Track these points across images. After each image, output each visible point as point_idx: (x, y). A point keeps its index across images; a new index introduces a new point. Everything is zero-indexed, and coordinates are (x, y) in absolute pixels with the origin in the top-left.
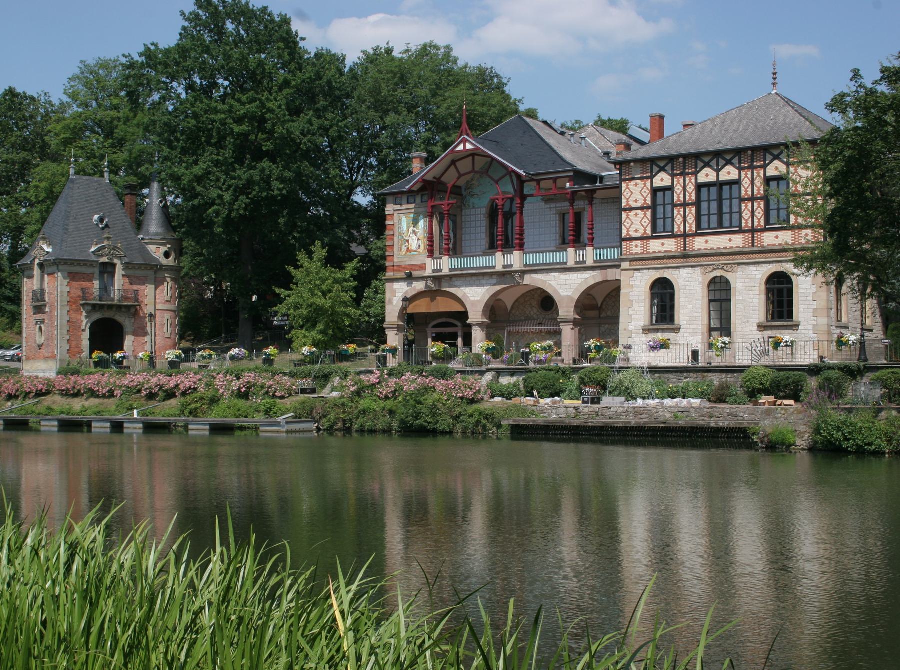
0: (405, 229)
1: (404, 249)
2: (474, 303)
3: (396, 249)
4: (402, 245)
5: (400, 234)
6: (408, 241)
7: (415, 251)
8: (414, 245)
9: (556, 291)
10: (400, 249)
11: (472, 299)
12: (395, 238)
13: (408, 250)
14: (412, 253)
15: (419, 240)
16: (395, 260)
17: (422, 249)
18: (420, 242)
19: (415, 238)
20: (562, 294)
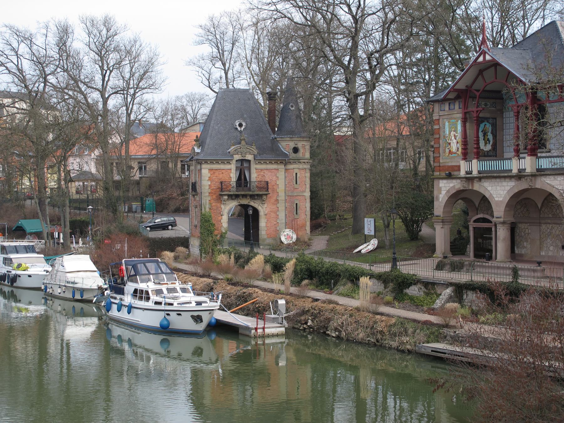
0: (448, 133)
1: (447, 151)
2: (498, 203)
4: (445, 147)
5: (444, 137)
6: (450, 144)
7: (455, 153)
11: (496, 199)
12: (441, 141)
13: (450, 152)
14: (453, 155)
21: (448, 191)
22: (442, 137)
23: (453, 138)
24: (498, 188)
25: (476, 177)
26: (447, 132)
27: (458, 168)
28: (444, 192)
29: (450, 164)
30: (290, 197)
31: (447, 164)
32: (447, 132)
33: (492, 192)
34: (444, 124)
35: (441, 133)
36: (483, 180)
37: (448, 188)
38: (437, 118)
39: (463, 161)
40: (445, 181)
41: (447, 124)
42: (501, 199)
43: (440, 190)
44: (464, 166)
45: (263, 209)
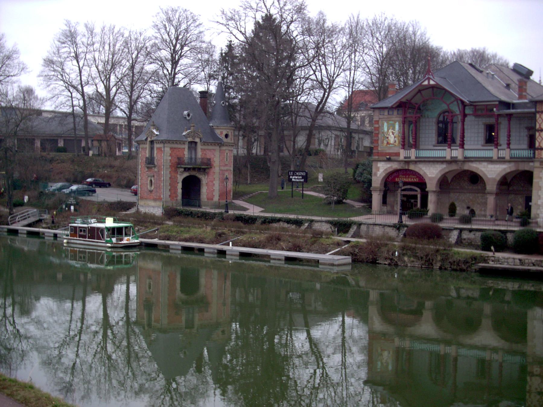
1: (385, 142)
2: (431, 179)
3: (379, 142)
4: (384, 140)
5: (383, 133)
6: (388, 138)
8: (392, 139)
9: (485, 174)
10: (383, 143)
11: (430, 176)
12: (380, 136)
13: (388, 143)
14: (391, 145)
16: (379, 149)
18: (396, 139)
19: (392, 136)
20: (489, 176)
21: (386, 170)
23: (391, 134)
24: (431, 169)
26: (386, 129)
27: (398, 154)
28: (381, 170)
29: (388, 151)
30: (222, 172)
32: (386, 129)
33: (426, 171)
35: (381, 131)
36: (418, 163)
37: (385, 168)
38: (378, 119)
39: (403, 150)
40: (383, 163)
41: (385, 124)
42: (434, 176)
43: (378, 169)
44: (403, 154)
45: (204, 179)
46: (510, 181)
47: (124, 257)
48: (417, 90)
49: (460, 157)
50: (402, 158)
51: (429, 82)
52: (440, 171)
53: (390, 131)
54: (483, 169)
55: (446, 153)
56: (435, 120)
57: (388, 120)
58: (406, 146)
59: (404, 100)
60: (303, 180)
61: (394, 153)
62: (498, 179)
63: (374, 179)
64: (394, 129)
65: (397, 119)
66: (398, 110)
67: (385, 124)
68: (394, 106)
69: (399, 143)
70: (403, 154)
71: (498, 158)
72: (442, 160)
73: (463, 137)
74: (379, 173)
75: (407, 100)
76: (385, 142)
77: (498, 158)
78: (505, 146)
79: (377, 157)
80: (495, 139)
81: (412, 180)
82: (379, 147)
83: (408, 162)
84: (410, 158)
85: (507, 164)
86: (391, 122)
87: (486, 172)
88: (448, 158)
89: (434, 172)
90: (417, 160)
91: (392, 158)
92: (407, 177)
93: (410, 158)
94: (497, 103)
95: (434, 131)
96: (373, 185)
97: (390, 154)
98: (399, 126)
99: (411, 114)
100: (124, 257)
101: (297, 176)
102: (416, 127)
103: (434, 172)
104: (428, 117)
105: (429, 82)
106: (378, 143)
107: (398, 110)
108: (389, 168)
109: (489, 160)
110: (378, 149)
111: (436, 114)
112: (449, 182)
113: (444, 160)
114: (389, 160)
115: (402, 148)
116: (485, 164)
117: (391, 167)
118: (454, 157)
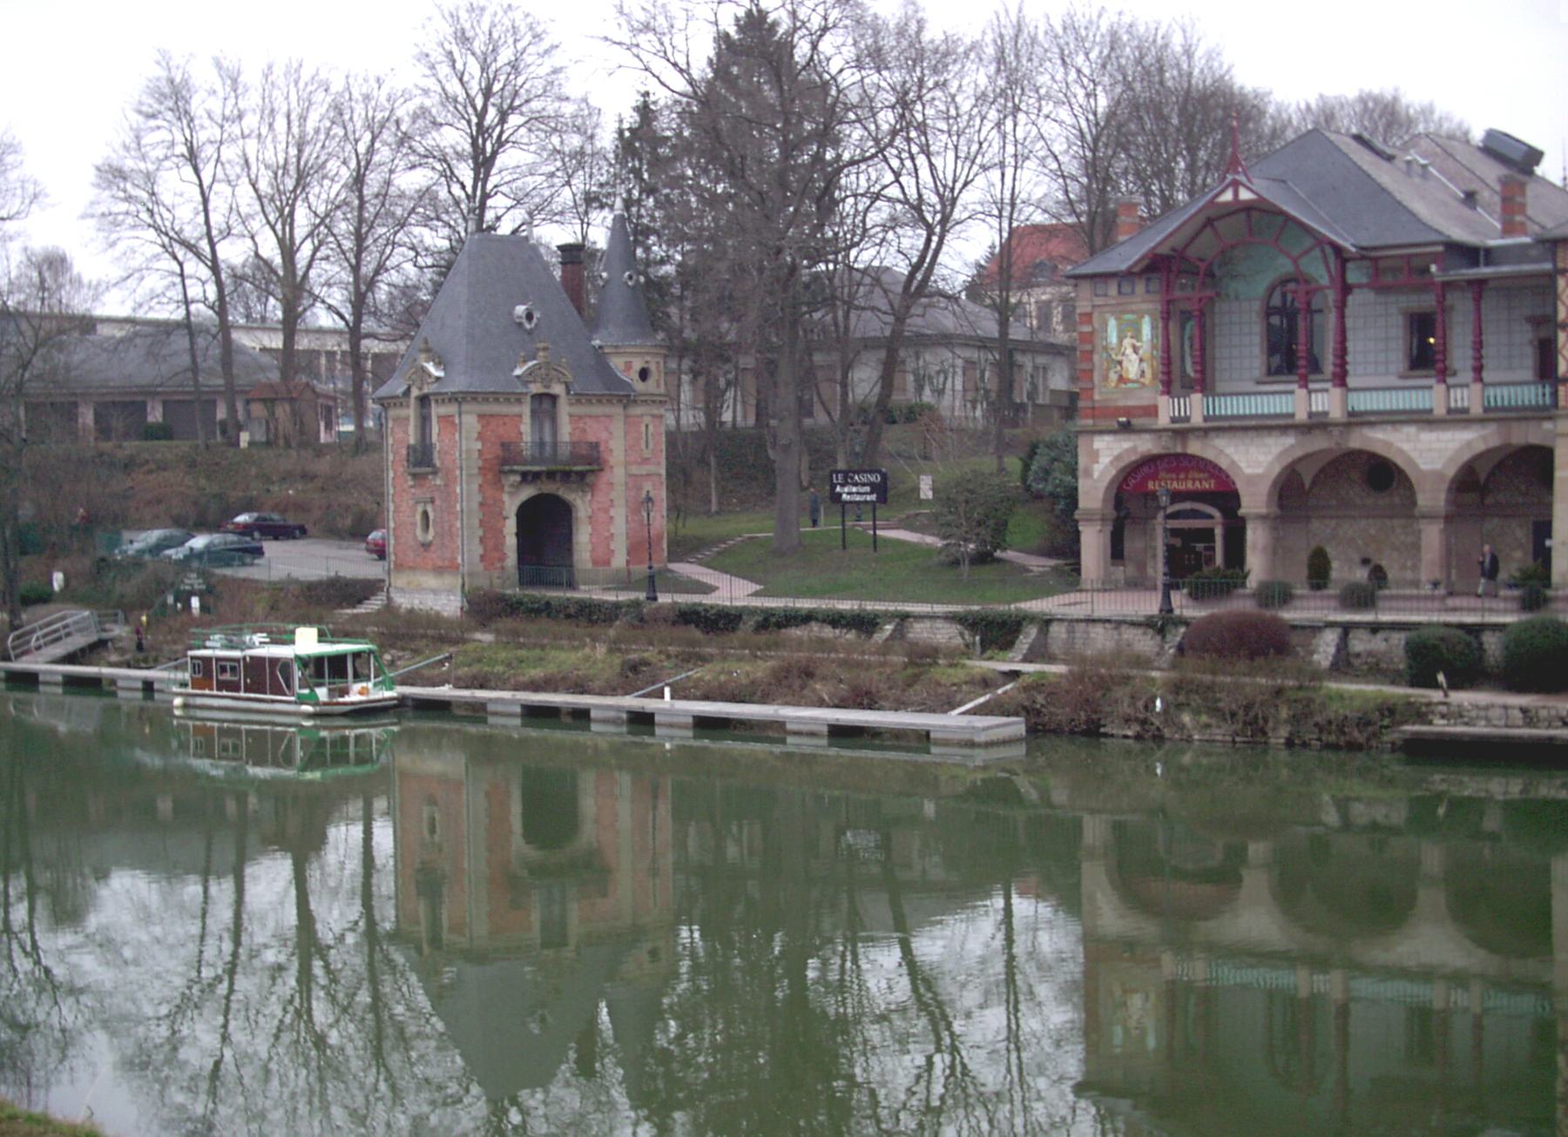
1: (1113, 377)
2: (1251, 480)
3: (1096, 377)
4: (1108, 369)
5: (1105, 348)
6: (1120, 363)
8: (1132, 368)
9: (1411, 461)
10: (1106, 378)
11: (1248, 471)
12: (1096, 358)
13: (1121, 379)
14: (1130, 385)
15: (1141, 360)
16: (1097, 397)
17: (1148, 379)
19: (1134, 357)
20: (1424, 467)
21: (1118, 458)
22: (1099, 348)
23: (1129, 351)
24: (1253, 450)
25: (1199, 429)
27: (1152, 411)
28: (1105, 460)
29: (1121, 403)
30: (634, 481)
31: (1112, 404)
33: (1236, 458)
34: (1106, 324)
35: (1098, 342)
36: (1212, 434)
37: (1116, 453)
38: (1088, 310)
39: (1166, 398)
40: (1108, 438)
41: (1112, 324)
42: (1260, 471)
43: (1095, 456)
44: (1167, 409)
45: (582, 505)
46: (1487, 479)
47: (352, 742)
48: (1201, 219)
49: (1336, 414)
50: (1163, 420)
51: (1236, 194)
52: (1281, 454)
53: (1127, 342)
54: (1406, 447)
55: (1293, 401)
56: (1257, 305)
57: (1118, 313)
58: (1176, 386)
59: (1164, 250)
60: (873, 497)
61: (1140, 407)
62: (1451, 472)
63: (1083, 485)
64: (1137, 335)
65: (1144, 306)
66: (1148, 280)
67: (1112, 324)
68: (1136, 270)
69: (1154, 376)
70: (1167, 409)
71: (1449, 411)
72: (1281, 422)
73: (1342, 352)
74: (1097, 470)
75: (1173, 249)
76: (1113, 377)
77: (1449, 411)
78: (1467, 376)
79: (1090, 422)
80: (1439, 357)
81: (1198, 484)
82: (1096, 391)
83: (1181, 432)
84: (1187, 419)
85: (1476, 427)
86: (1128, 317)
87: (1414, 455)
88: (1301, 416)
89: (1261, 458)
90: (1209, 424)
91: (1136, 422)
92: (1182, 476)
93: (1187, 419)
94: (1440, 249)
95: (1257, 340)
96: (1081, 504)
97: (1128, 411)
98: (1153, 328)
99: (1187, 291)
100: (352, 742)
101: (856, 484)
102: (1202, 327)
103: (1261, 458)
104: (1237, 298)
105: (1236, 194)
106: (1091, 380)
107: (1148, 280)
108: (1127, 450)
109: (1424, 419)
110: (1091, 398)
111: (1260, 286)
112: (1307, 483)
113: (1289, 421)
114: (1126, 428)
115: (1163, 393)
116: (1411, 430)
117: (1134, 449)
118: (1318, 414)
